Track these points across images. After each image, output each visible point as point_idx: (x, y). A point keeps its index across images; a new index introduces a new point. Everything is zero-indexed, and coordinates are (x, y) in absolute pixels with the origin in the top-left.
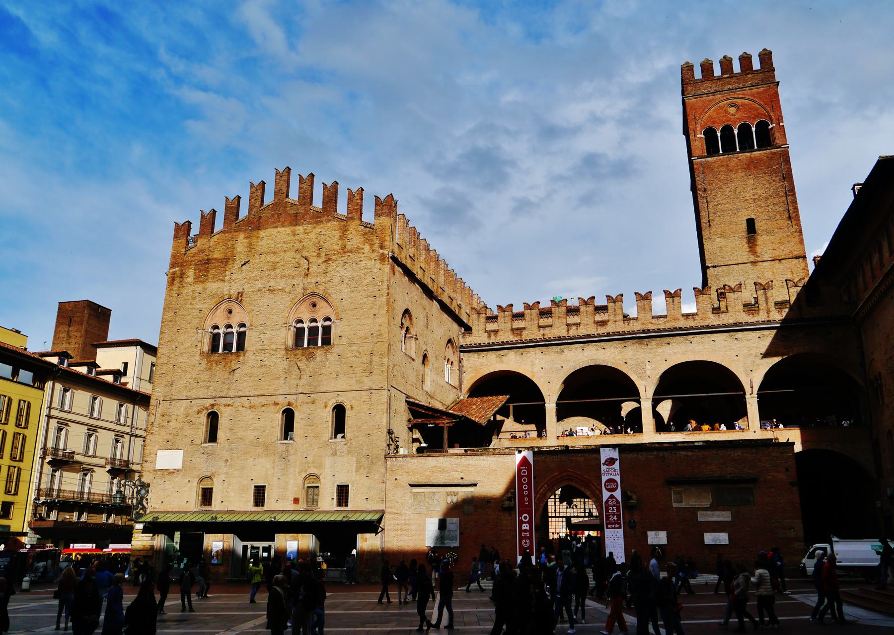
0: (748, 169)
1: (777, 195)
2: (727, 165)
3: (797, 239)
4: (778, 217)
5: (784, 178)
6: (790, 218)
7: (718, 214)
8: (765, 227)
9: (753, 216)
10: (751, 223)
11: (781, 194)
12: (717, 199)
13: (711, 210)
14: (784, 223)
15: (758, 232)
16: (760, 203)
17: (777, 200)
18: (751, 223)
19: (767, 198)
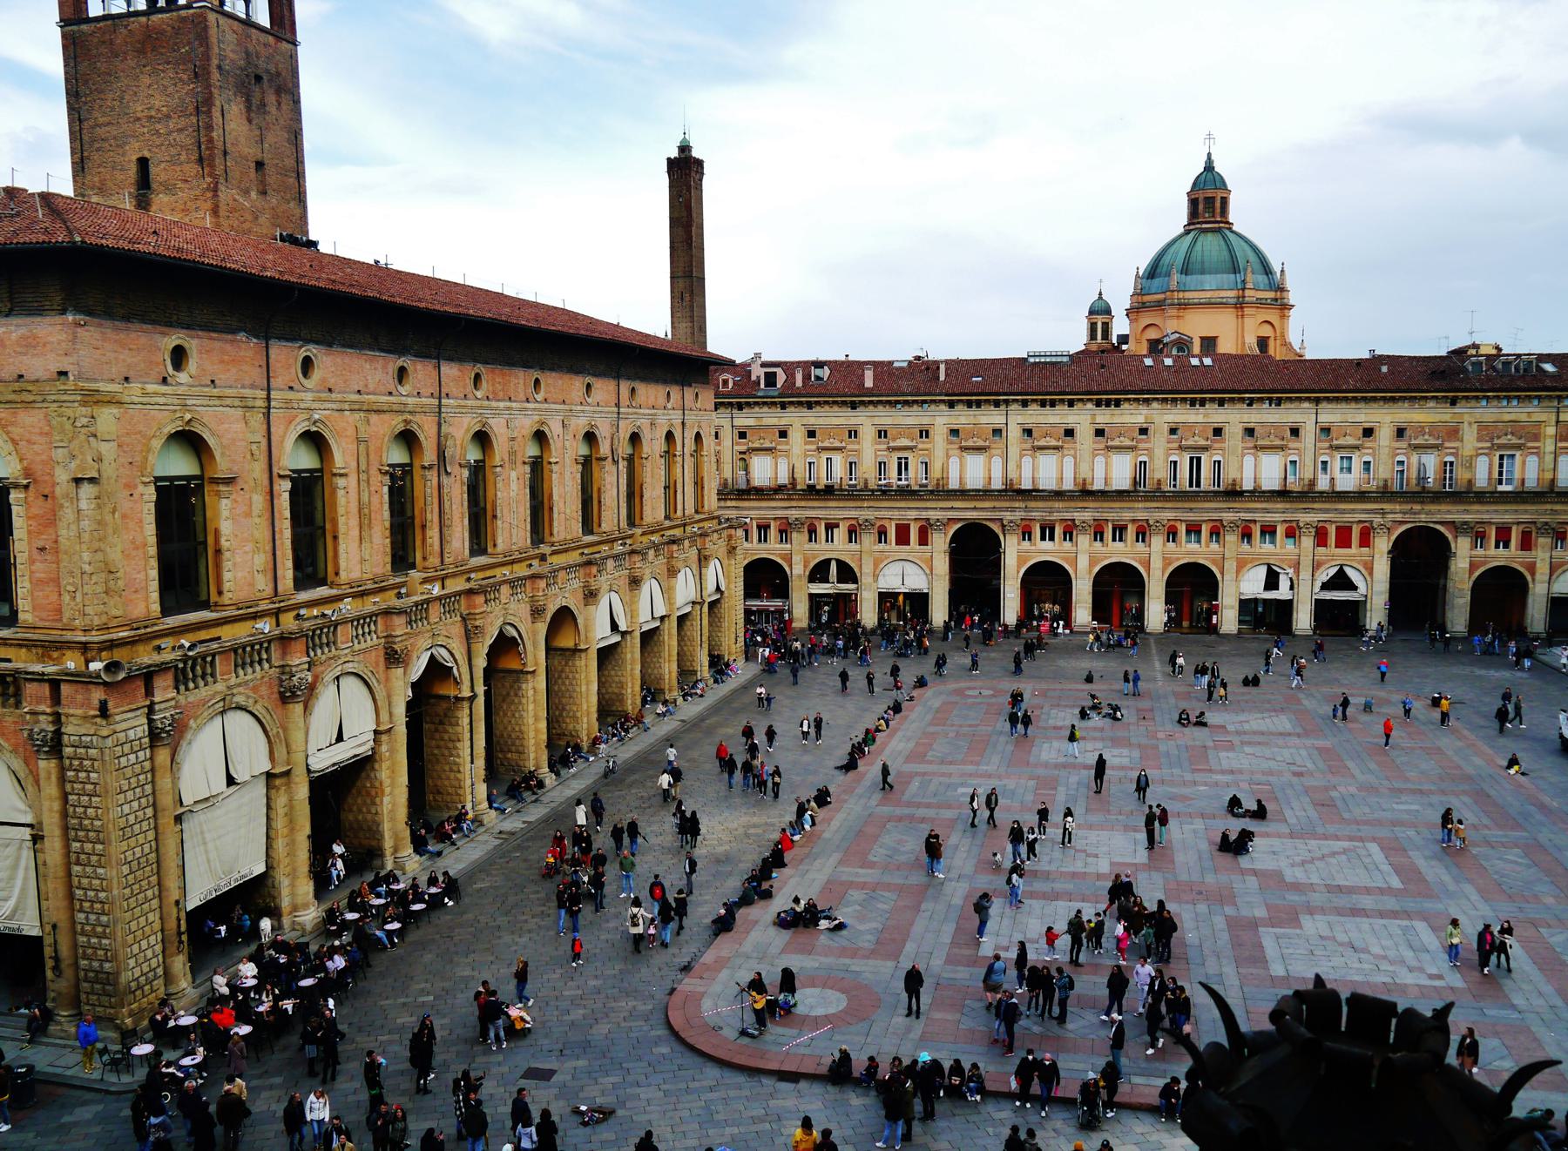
0: (141, 52)
1: (183, 113)
2: (111, 42)
3: (209, 205)
4: (183, 158)
5: (196, 75)
6: (200, 160)
7: (97, 145)
8: (163, 177)
9: (147, 154)
10: (143, 163)
11: (191, 109)
12: (96, 114)
13: (85, 138)
14: (192, 169)
15: (154, 186)
16: (158, 126)
17: (182, 122)
18: (143, 163)
19: (168, 117)
